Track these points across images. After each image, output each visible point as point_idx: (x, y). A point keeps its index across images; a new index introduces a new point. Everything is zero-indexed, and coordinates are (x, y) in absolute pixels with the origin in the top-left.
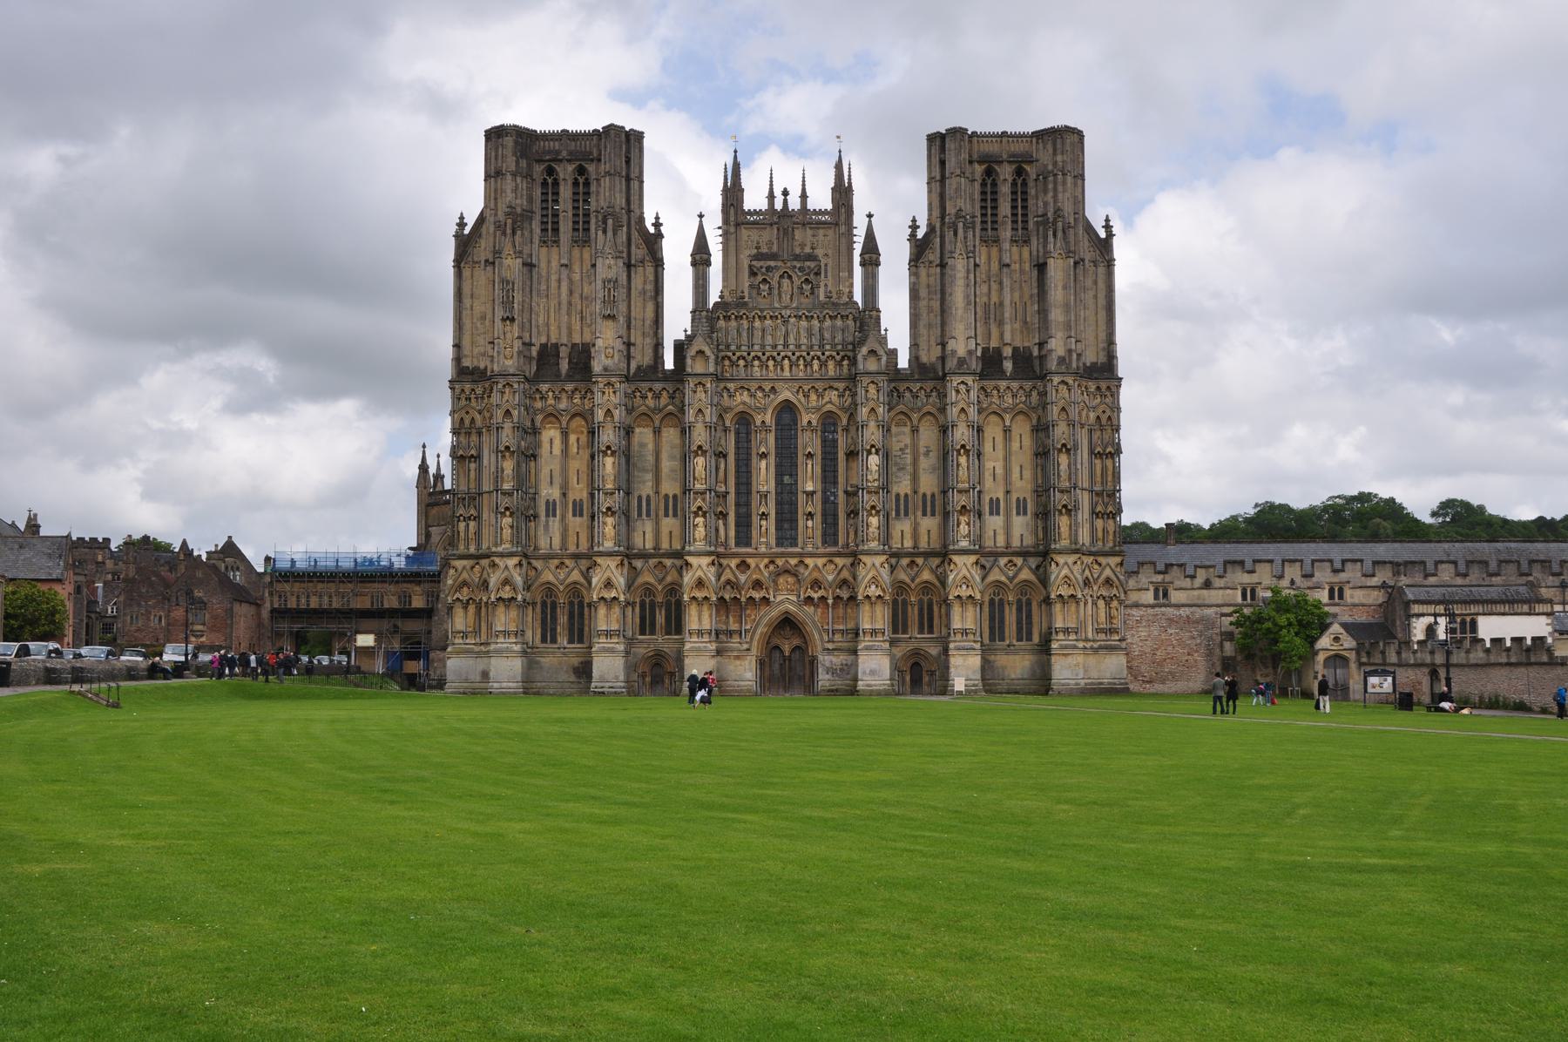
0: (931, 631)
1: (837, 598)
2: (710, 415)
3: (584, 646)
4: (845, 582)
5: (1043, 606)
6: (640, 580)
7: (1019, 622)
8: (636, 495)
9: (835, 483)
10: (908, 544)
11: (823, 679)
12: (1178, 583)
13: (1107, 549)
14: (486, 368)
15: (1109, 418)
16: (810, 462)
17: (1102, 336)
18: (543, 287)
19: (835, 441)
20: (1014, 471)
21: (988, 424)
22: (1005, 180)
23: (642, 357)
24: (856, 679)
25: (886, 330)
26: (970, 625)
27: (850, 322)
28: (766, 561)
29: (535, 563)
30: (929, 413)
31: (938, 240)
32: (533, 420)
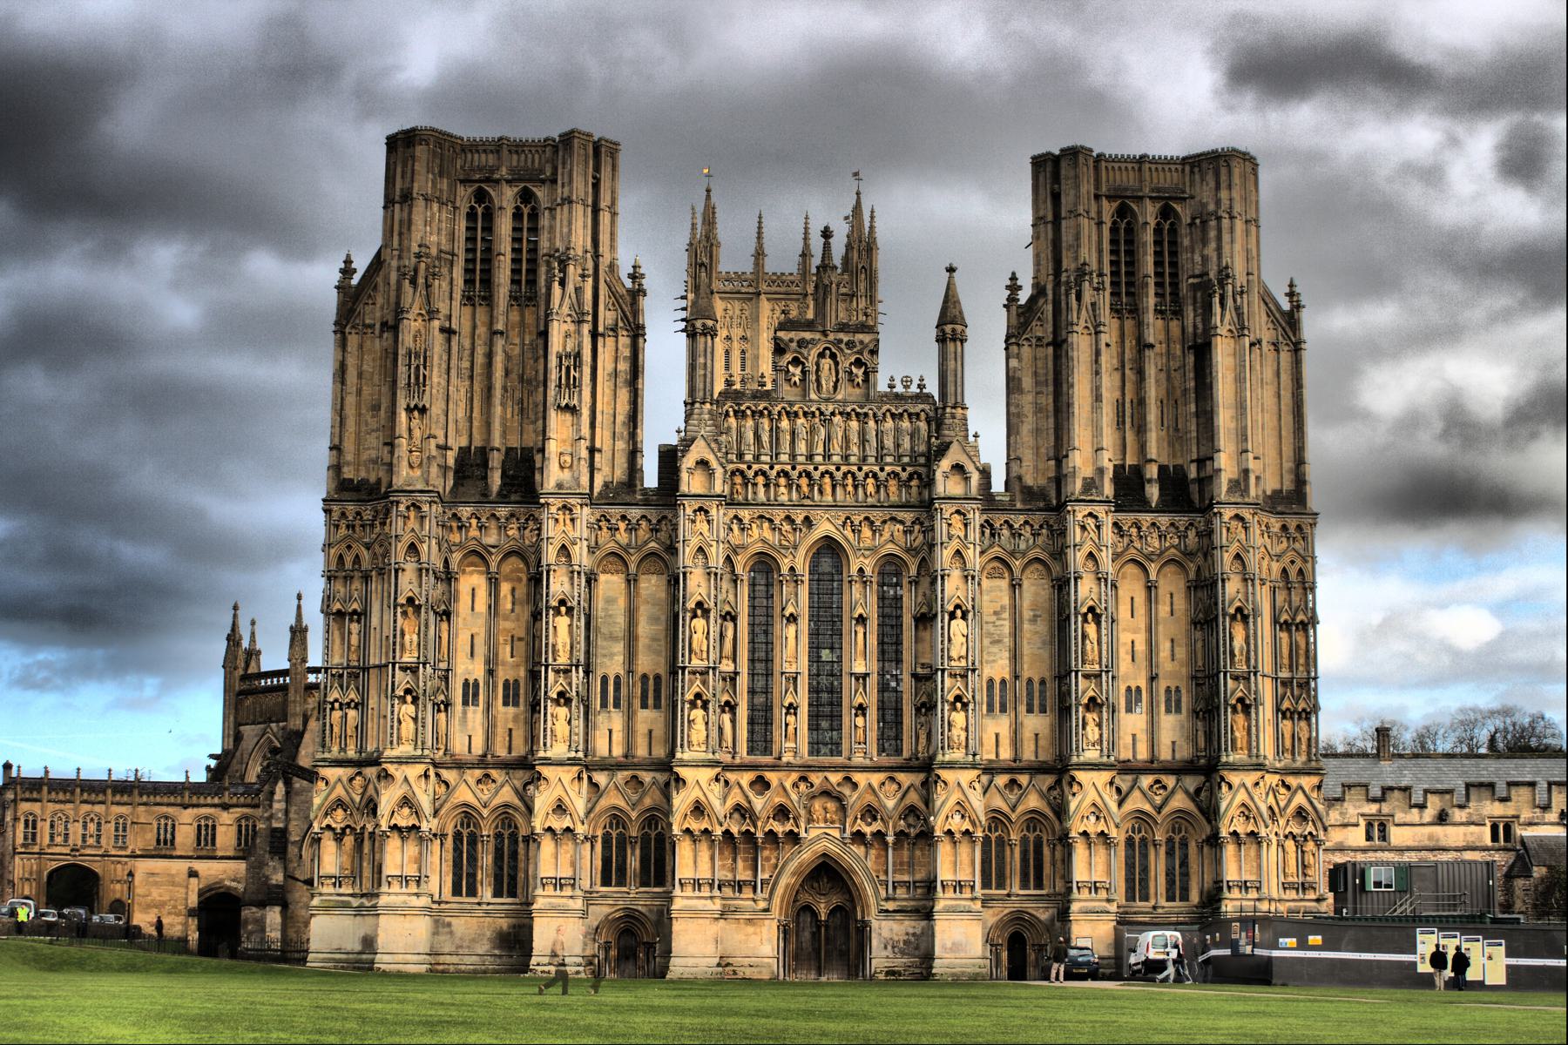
0: (1039, 885)
1: (900, 835)
2: (717, 556)
3: (517, 900)
4: (912, 810)
5: (1206, 849)
6: (604, 803)
7: (1170, 874)
8: (599, 673)
9: (899, 661)
10: (1006, 754)
11: (880, 958)
12: (1399, 817)
13: (1298, 764)
14: (379, 481)
15: (1301, 572)
16: (860, 630)
17: (1288, 450)
18: (466, 364)
19: (898, 599)
20: (1161, 647)
22: (1146, 223)
23: (610, 470)
24: (928, 957)
25: (976, 436)
26: (1098, 875)
27: (923, 425)
28: (794, 776)
29: (446, 774)
30: (1037, 560)
31: (1050, 307)
32: (446, 562)
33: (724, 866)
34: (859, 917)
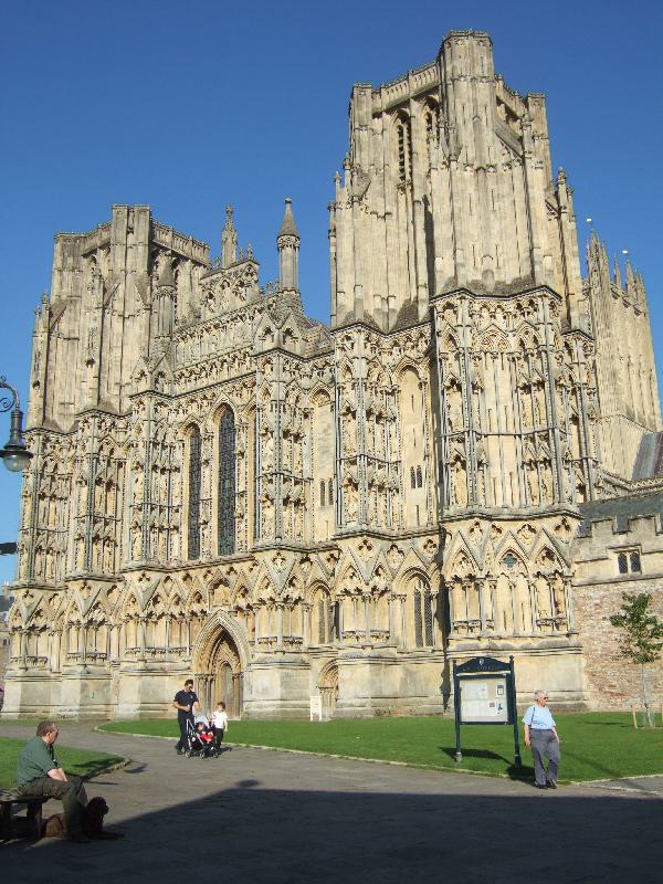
15: (535, 340)
17: (525, 244)
21: (406, 381)
28: (204, 570)
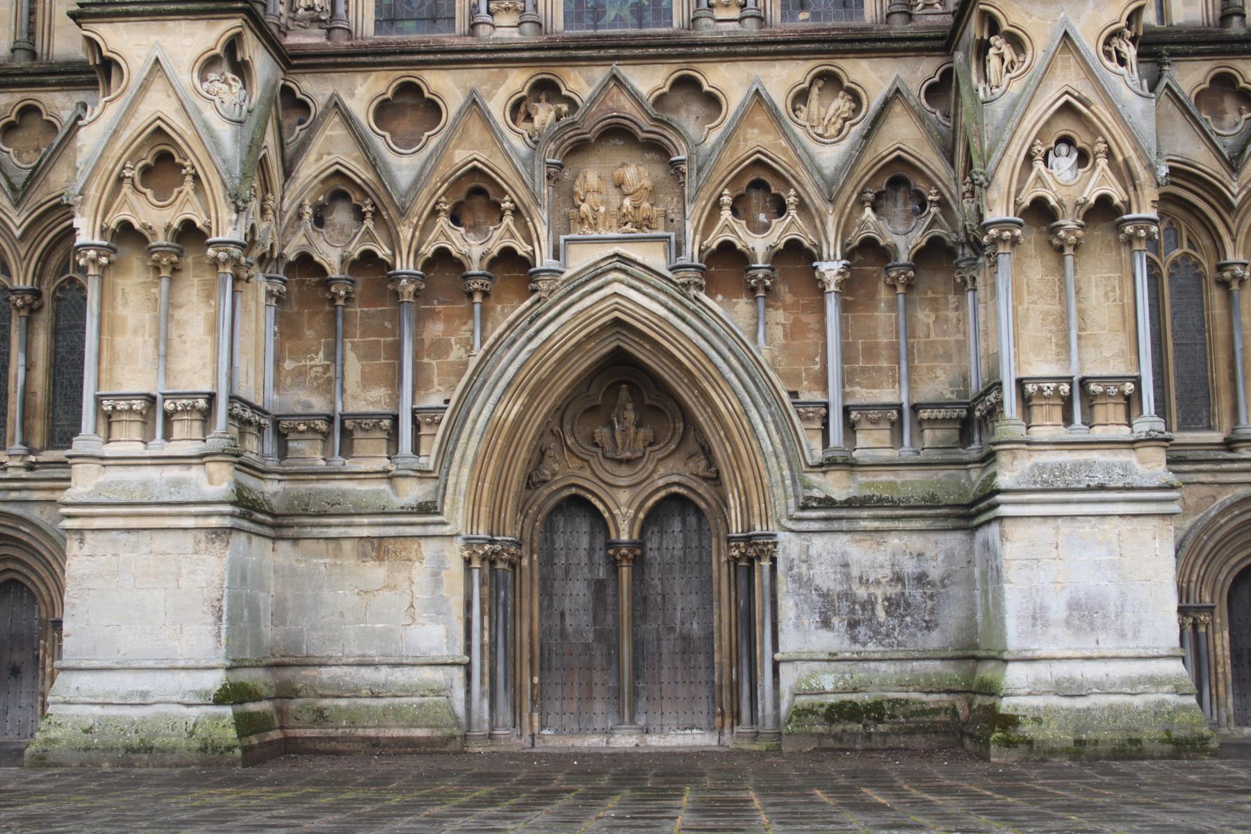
28: (517, 80)
33: (300, 373)
34: (736, 529)
